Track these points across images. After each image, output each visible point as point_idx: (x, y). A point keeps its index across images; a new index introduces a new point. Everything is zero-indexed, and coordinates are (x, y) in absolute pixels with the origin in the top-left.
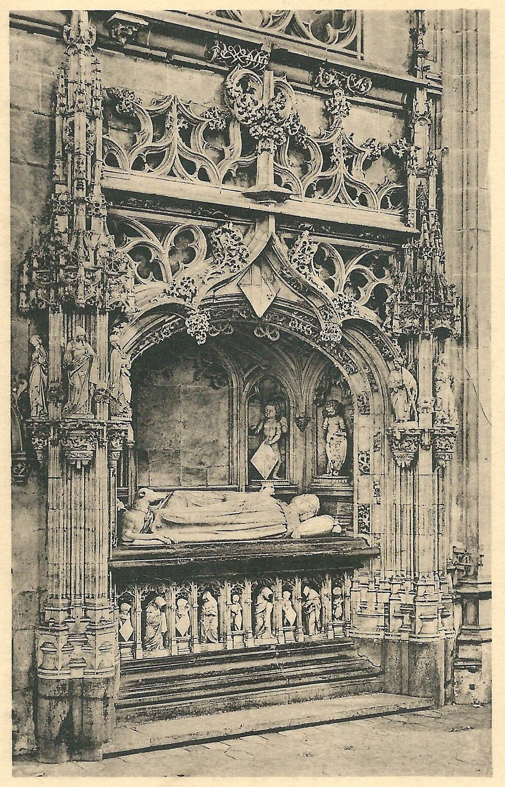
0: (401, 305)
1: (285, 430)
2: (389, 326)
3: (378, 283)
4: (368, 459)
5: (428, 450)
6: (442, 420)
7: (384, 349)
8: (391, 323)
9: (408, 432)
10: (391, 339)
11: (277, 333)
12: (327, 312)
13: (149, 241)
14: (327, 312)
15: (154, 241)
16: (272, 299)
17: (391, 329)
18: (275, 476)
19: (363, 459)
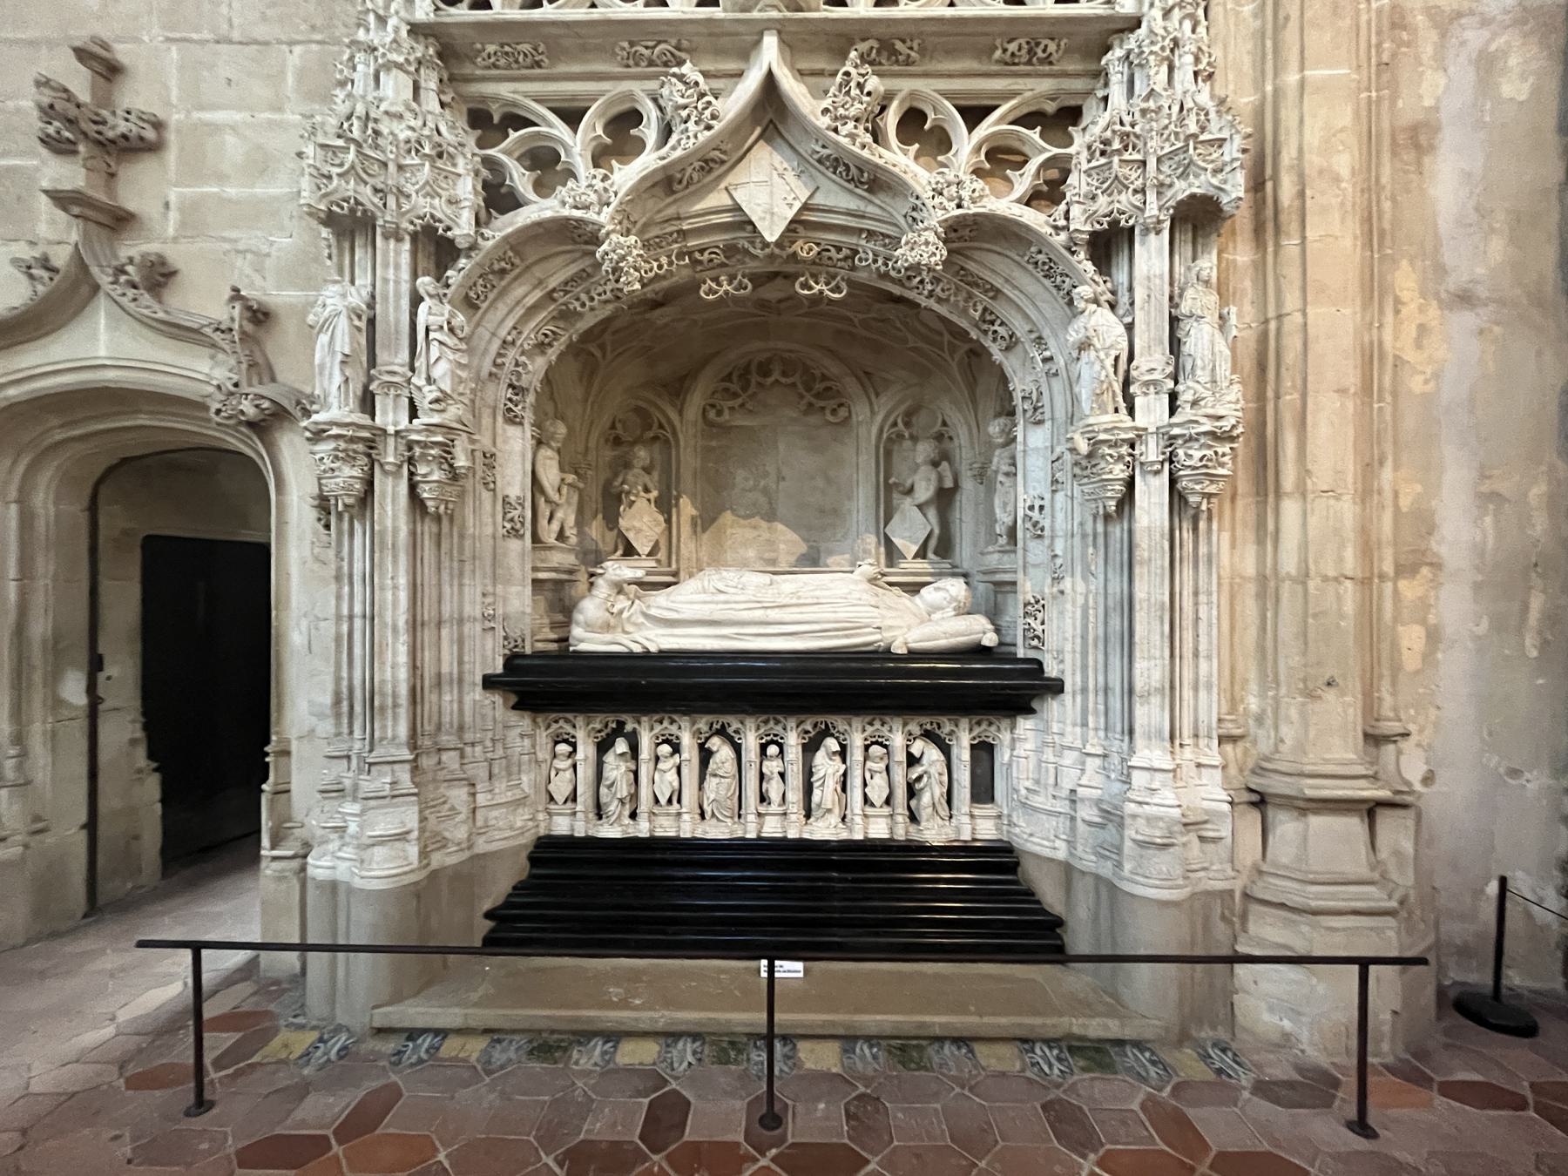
0: (1088, 173)
1: (949, 484)
2: (1062, 223)
3: (1047, 155)
4: (1042, 508)
5: (1157, 473)
6: (1194, 403)
7: (1059, 279)
8: (1067, 218)
9: (1102, 437)
10: (1069, 249)
11: (844, 285)
12: (914, 214)
13: (554, 132)
14: (914, 214)
15: (560, 129)
16: (797, 205)
17: (1066, 228)
18: (931, 555)
19: (1031, 508)
